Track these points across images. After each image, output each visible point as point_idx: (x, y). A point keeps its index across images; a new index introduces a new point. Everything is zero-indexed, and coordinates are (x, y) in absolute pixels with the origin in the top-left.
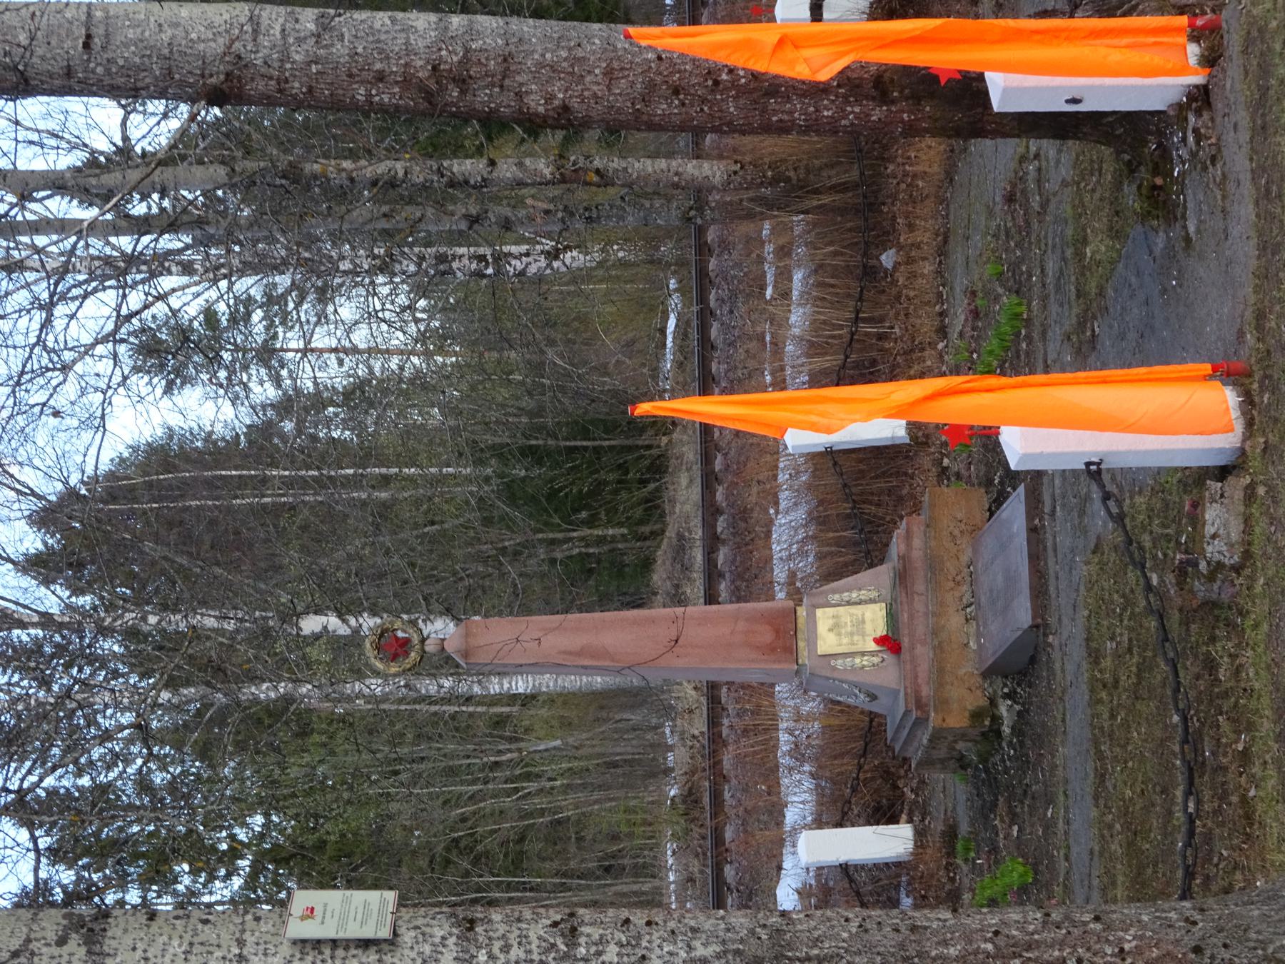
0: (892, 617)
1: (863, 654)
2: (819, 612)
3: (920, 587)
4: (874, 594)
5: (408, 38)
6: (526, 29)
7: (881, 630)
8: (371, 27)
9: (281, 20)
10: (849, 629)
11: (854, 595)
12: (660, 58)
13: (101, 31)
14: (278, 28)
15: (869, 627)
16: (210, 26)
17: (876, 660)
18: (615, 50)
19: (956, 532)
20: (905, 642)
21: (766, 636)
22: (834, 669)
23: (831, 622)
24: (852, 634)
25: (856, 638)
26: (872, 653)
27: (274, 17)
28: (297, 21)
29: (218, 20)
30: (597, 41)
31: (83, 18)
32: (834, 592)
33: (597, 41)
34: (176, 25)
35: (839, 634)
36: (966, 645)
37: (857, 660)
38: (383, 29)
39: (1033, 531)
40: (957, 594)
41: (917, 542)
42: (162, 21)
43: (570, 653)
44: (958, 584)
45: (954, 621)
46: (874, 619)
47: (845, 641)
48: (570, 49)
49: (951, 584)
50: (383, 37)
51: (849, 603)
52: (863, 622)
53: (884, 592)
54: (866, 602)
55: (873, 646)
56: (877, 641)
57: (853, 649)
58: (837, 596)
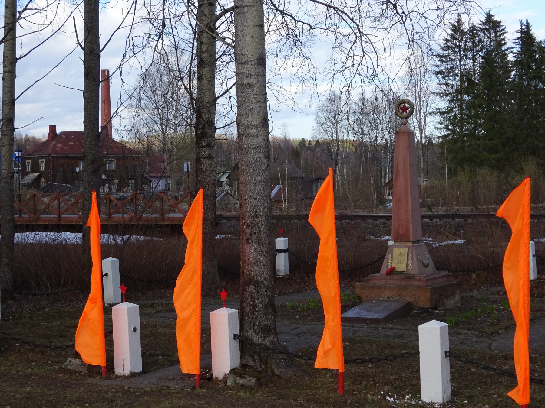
0: (401, 273)
2: (406, 249)
3: (403, 283)
5: (243, 115)
6: (252, 154)
8: (247, 102)
9: (247, 72)
12: (246, 200)
13: (240, 11)
14: (244, 71)
15: (399, 265)
16: (243, 48)
18: (247, 185)
19: (416, 296)
20: (391, 277)
21: (401, 232)
22: (389, 253)
27: (248, 69)
28: (247, 77)
29: (245, 50)
30: (250, 179)
31: (244, 5)
32: (412, 255)
33: (250, 179)
34: (243, 37)
36: (380, 297)
38: (247, 107)
39: (366, 319)
40: (396, 295)
41: (417, 283)
42: (244, 31)
43: (397, 167)
44: (399, 295)
45: (388, 293)
46: (401, 267)
48: (246, 170)
49: (399, 293)
50: (244, 107)
51: (408, 259)
52: (401, 263)
57: (394, 260)
58: (411, 255)
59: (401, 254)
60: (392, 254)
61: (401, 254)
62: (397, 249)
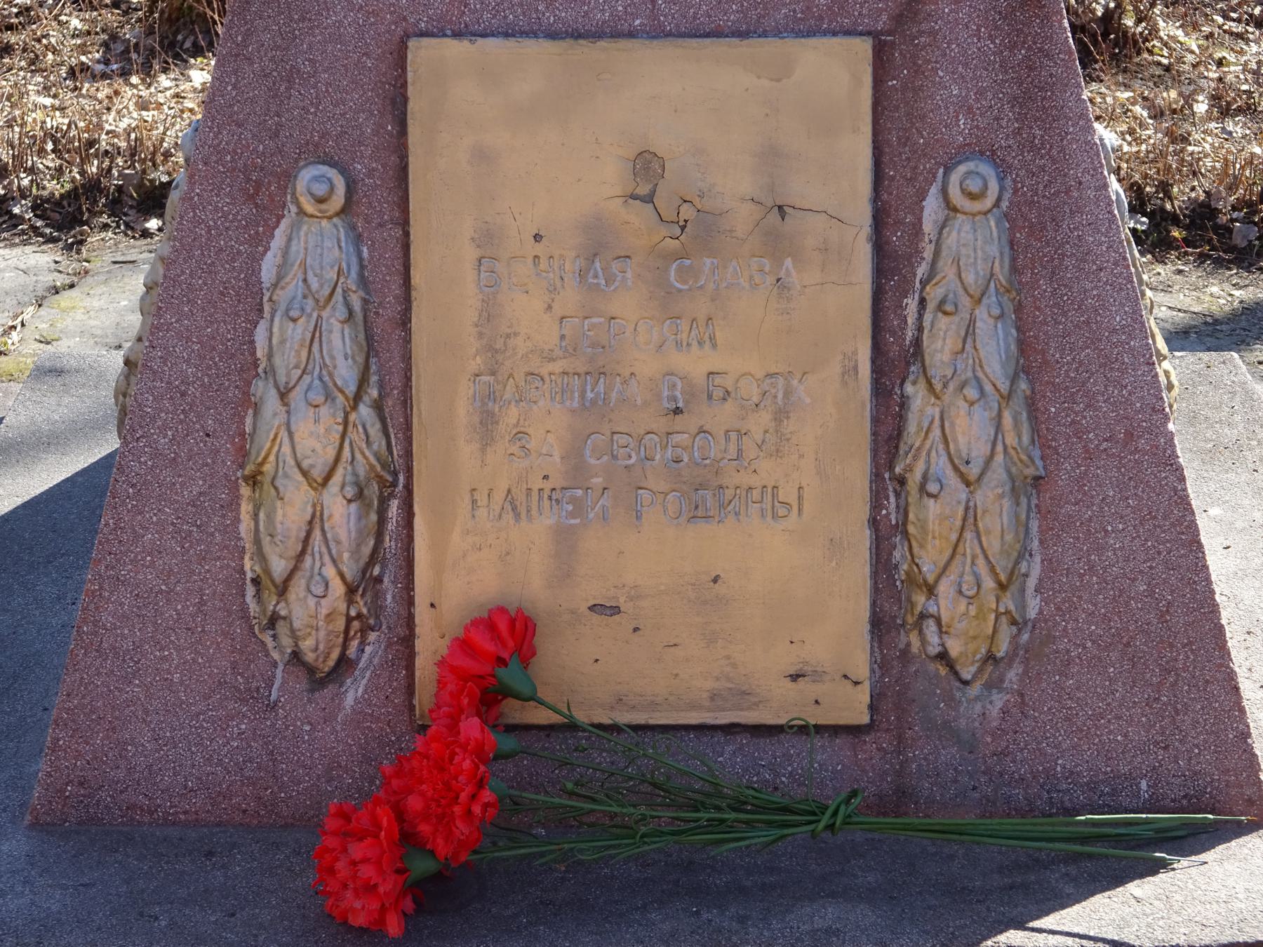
1: (390, 490)
4: (960, 618)
7: (596, 672)
10: (651, 355)
11: (971, 430)
15: (646, 555)
17: (314, 612)
23: (734, 188)
24: (592, 372)
25: (548, 428)
26: (383, 577)
35: (598, 247)
37: (314, 434)
47: (533, 318)
51: (893, 362)
52: (703, 495)
53: (983, 708)
54: (887, 534)
55: (456, 575)
56: (502, 640)
59: (671, 226)
60: (383, 205)
61: (671, 226)
62: (533, 64)
